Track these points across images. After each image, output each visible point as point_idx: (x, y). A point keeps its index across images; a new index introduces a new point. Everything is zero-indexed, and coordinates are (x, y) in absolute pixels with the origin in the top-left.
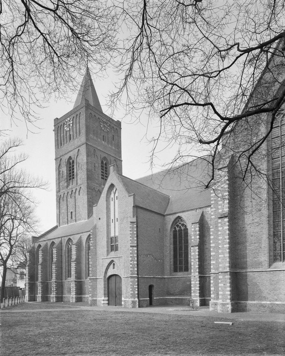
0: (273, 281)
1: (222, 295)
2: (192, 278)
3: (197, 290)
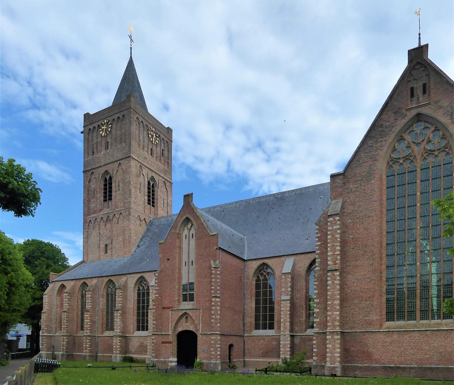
3: (288, 351)
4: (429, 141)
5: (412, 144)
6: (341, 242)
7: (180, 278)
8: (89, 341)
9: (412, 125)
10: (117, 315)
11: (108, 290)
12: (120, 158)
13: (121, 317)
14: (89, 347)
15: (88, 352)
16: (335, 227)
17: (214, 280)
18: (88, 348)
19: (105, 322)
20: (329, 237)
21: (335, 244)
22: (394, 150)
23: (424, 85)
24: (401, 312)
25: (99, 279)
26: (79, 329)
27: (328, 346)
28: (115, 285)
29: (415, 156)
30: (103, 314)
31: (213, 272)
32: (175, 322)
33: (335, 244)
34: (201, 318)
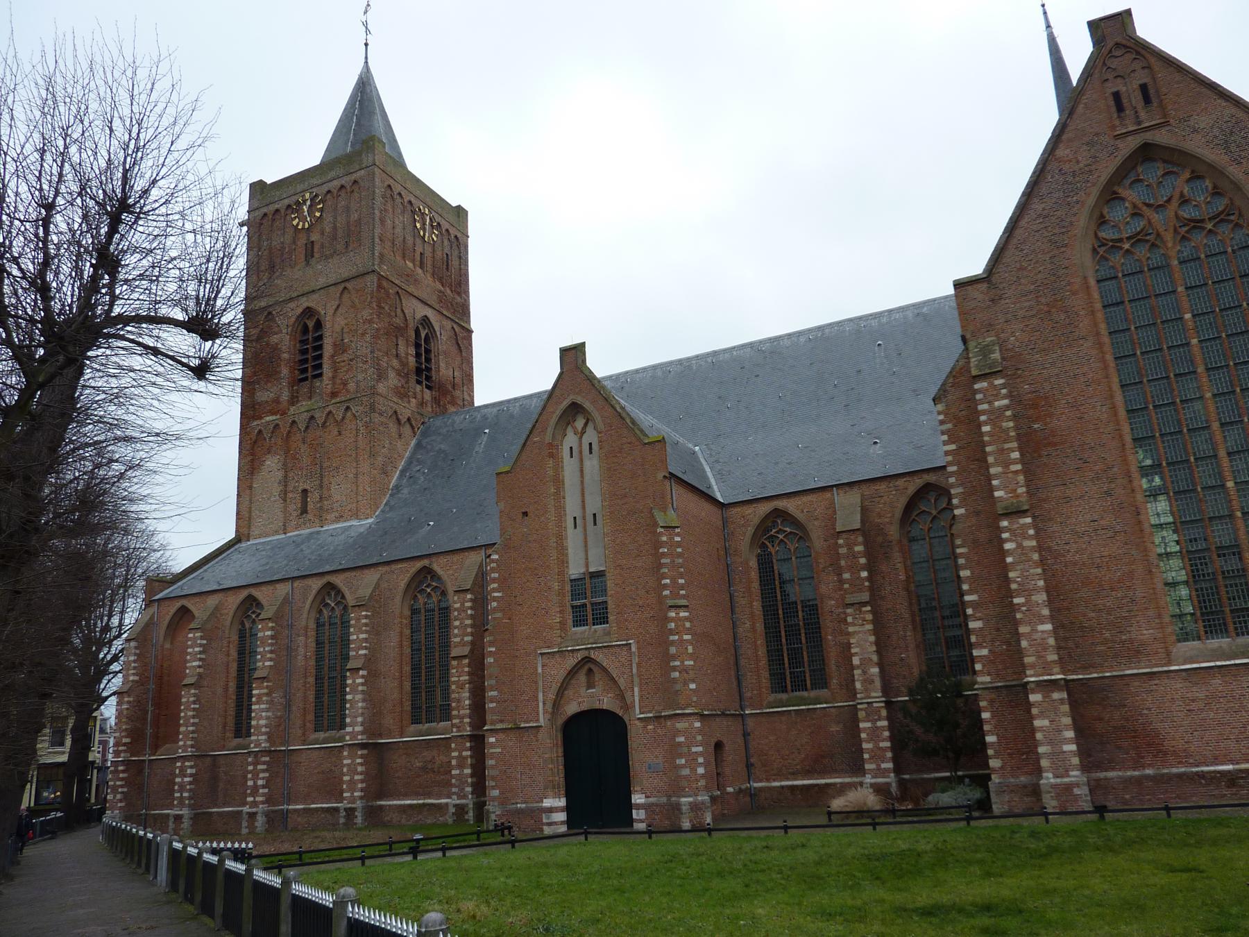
0: (1193, 701)
1: (1051, 755)
2: (861, 709)
4: (1184, 201)
5: (1145, 208)
6: (1019, 438)
7: (563, 562)
8: (264, 767)
9: (1134, 167)
10: (354, 682)
11: (320, 612)
12: (346, 275)
13: (365, 688)
14: (263, 787)
15: (263, 803)
16: (997, 404)
17: (668, 561)
18: (261, 791)
19: (311, 707)
20: (986, 429)
21: (1007, 446)
22: (1102, 221)
23: (1144, 88)
24: (1212, 613)
25: (295, 585)
26: (229, 735)
27: (1037, 723)
28: (343, 597)
29: (1158, 235)
30: (305, 682)
31: (664, 539)
32: (555, 687)
33: (1007, 446)
34: (635, 670)
